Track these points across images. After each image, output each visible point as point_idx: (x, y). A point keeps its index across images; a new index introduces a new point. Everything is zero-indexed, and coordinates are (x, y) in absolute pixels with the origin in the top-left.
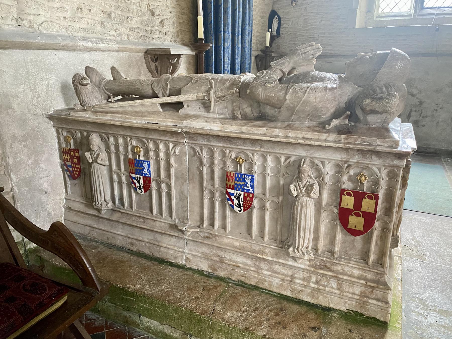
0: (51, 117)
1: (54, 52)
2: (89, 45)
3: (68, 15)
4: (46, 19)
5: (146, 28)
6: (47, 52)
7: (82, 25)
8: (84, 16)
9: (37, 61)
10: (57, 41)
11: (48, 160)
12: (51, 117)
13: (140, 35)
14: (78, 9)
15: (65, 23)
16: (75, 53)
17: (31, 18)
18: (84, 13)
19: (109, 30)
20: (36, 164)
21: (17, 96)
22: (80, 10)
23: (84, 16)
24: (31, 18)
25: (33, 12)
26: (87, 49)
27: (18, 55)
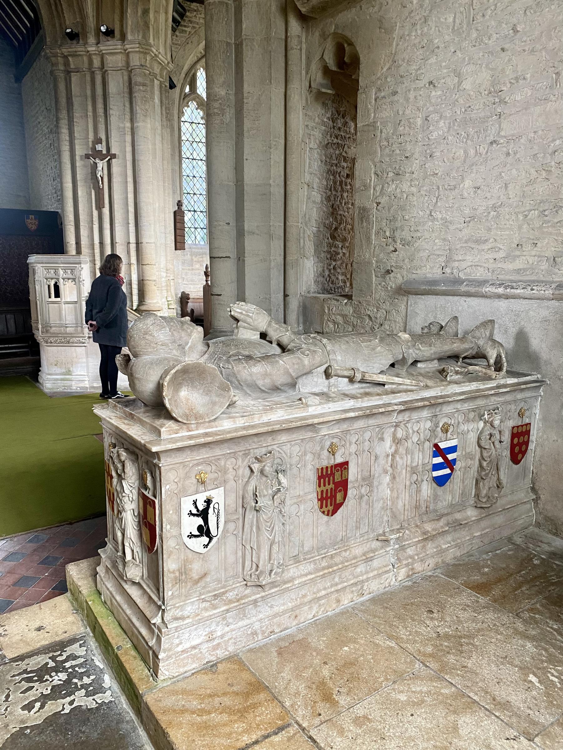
1: (464, 298)
2: (501, 290)
3: (502, 254)
4: (472, 264)
6: (456, 298)
7: (519, 264)
8: (525, 253)
16: (488, 301)
18: (524, 249)
22: (520, 247)
23: (525, 253)
24: (456, 264)
25: (460, 258)
26: (499, 296)
27: (431, 300)
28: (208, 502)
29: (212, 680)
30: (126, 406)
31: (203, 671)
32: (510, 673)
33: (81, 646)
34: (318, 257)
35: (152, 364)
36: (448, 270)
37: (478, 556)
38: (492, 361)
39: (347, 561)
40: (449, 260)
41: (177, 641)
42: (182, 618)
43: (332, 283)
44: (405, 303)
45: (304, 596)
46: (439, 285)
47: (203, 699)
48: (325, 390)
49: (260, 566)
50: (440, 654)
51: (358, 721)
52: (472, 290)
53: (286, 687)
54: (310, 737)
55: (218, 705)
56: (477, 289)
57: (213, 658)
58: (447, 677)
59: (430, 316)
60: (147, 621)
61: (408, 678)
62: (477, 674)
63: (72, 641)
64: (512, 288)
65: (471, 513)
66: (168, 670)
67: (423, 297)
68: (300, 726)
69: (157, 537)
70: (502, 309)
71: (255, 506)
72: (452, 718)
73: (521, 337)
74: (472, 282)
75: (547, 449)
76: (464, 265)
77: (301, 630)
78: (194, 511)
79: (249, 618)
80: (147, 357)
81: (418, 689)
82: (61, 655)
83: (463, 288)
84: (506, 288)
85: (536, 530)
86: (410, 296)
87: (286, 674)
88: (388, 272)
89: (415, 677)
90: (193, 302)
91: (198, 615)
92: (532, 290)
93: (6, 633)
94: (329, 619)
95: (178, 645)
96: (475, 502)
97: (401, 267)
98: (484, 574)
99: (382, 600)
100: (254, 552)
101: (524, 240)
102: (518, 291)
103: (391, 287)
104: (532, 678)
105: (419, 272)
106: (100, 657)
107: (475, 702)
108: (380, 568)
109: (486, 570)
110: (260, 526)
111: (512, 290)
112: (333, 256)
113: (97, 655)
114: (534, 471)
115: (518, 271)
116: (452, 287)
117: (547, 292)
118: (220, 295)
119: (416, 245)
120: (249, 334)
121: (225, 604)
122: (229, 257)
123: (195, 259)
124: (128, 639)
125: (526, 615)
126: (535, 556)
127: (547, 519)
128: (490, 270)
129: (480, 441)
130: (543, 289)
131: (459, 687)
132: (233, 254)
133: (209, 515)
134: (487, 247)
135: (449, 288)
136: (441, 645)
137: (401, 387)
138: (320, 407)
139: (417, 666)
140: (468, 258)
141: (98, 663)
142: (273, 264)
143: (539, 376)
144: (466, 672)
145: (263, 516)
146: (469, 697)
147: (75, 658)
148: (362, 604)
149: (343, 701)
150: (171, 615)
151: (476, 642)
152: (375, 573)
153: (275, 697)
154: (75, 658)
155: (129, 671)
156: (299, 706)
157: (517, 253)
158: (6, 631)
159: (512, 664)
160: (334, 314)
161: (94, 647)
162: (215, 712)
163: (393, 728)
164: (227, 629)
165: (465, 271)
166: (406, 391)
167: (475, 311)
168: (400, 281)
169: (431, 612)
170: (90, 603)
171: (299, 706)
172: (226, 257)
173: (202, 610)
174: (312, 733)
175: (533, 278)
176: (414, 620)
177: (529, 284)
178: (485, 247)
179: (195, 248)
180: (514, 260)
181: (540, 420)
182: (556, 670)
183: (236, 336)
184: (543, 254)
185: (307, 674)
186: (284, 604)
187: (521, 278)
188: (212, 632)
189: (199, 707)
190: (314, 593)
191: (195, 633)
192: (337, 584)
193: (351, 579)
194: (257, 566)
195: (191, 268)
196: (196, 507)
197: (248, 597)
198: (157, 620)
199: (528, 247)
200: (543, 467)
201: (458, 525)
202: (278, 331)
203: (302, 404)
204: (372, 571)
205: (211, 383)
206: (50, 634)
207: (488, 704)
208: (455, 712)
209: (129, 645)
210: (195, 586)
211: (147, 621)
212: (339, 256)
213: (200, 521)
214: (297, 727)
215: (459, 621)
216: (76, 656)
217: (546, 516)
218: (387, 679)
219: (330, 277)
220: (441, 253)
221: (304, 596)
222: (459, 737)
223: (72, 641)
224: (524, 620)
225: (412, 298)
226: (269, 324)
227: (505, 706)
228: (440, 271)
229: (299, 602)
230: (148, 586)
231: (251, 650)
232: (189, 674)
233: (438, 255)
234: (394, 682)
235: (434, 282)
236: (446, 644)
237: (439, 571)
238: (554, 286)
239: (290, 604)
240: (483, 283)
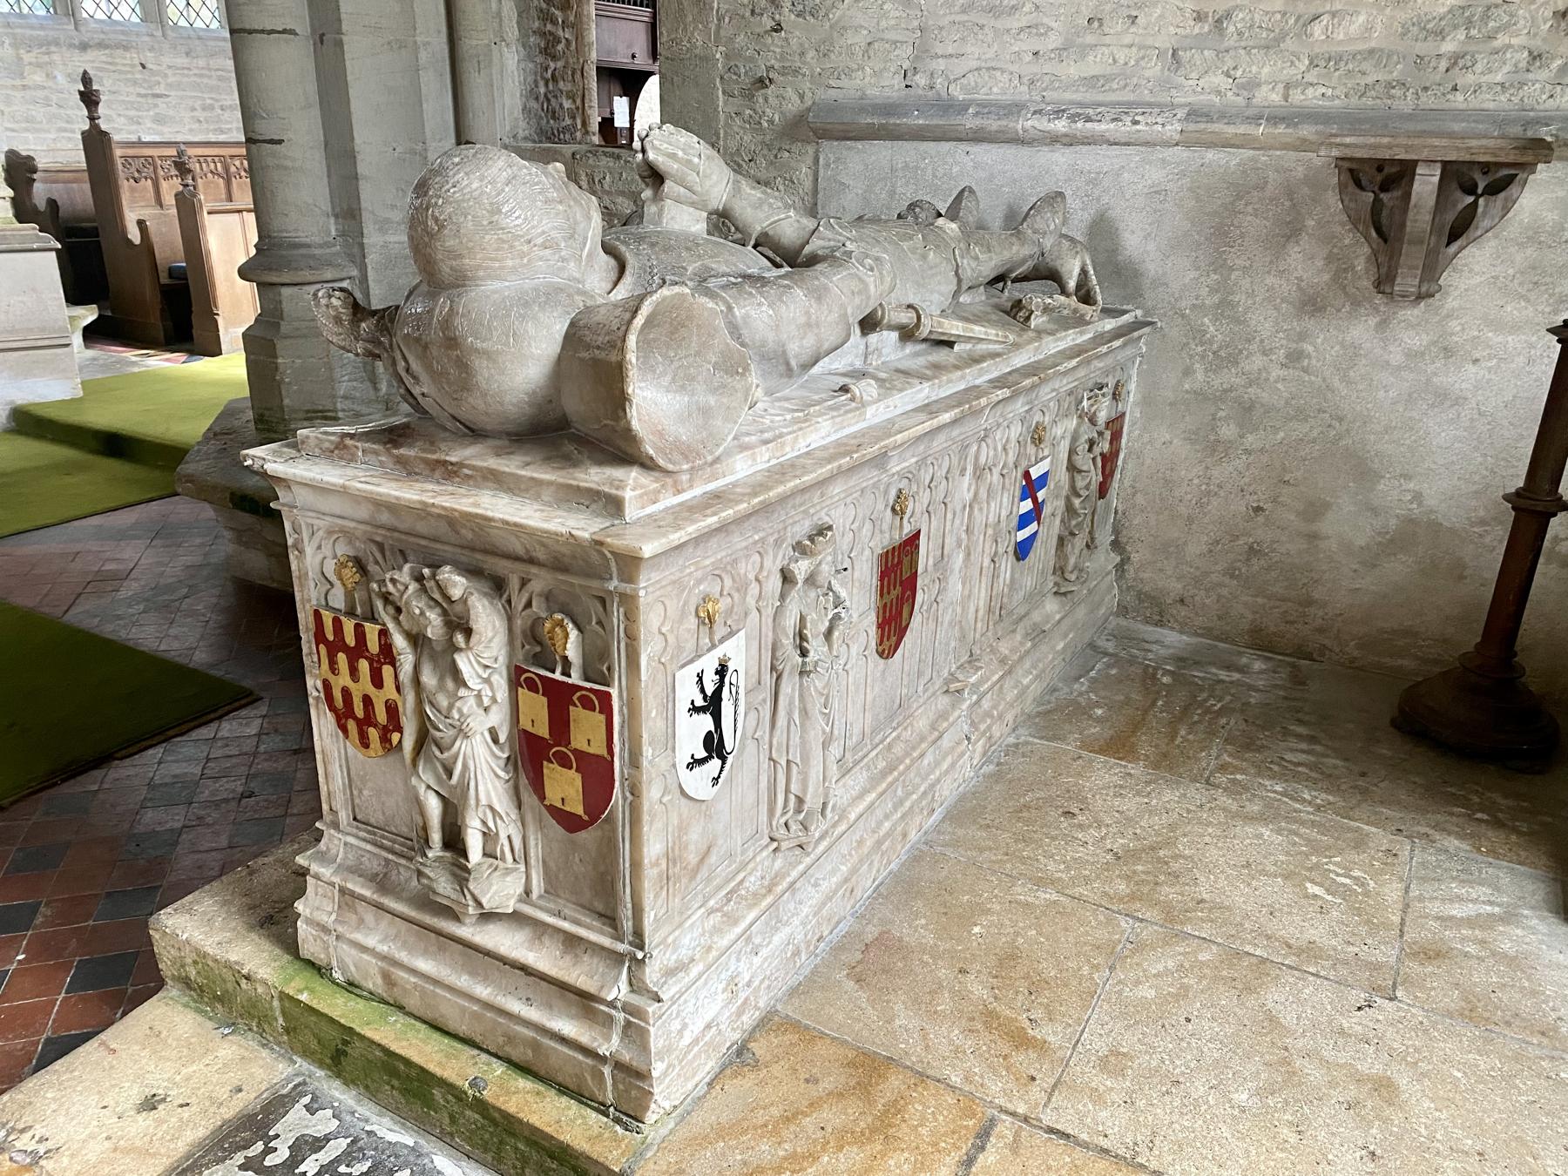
1: (964, 146)
2: (1061, 126)
3: (1054, 41)
4: (980, 66)
6: (945, 146)
7: (1094, 65)
8: (1107, 40)
9: (917, 168)
10: (958, 120)
13: (1370, 80)
18: (1107, 30)
19: (1194, 75)
22: (1096, 24)
24: (941, 64)
25: (950, 51)
26: (1054, 140)
27: (881, 153)
28: (722, 671)
29: (762, 1083)
30: (397, 445)
31: (728, 1071)
32: (1274, 890)
33: (310, 1109)
34: (524, 46)
35: (526, 304)
36: (921, 80)
37: (1066, 690)
38: (1072, 284)
39: (914, 748)
40: (922, 52)
41: (676, 1025)
42: (681, 967)
43: (554, 118)
44: (809, 161)
45: (860, 842)
46: (905, 115)
47: (776, 1131)
48: (858, 364)
49: (808, 798)
50: (1146, 890)
51: (1114, 1062)
52: (993, 124)
53: (927, 1046)
54: (1051, 1130)
55: (820, 1134)
56: (1004, 123)
57: (737, 1036)
58: (1188, 929)
59: (877, 190)
60: (585, 1002)
61: (1126, 953)
62: (1228, 908)
63: (276, 1106)
64: (1089, 120)
65: (1052, 606)
66: (667, 1098)
67: (859, 145)
68: (1013, 1114)
69: (617, 784)
70: (1057, 169)
71: (804, 664)
72: (1251, 1001)
73: (1102, 233)
74: (986, 108)
75: (1148, 461)
77: (863, 916)
78: (700, 702)
79: (787, 924)
80: (497, 285)
81: (1160, 967)
82: (269, 1151)
83: (970, 122)
84: (1073, 118)
85: (1123, 622)
86: (825, 143)
87: (904, 1018)
88: (762, 83)
89: (1139, 947)
90: (45, 181)
91: (709, 949)
92: (1136, 123)
93: (49, 1145)
94: (896, 877)
95: (680, 1032)
96: (1056, 584)
97: (796, 72)
98: (1099, 720)
99: (964, 812)
100: (794, 769)
101: (1108, 7)
102: (1103, 127)
103: (771, 122)
104: (1313, 889)
105: (845, 82)
106: (386, 1121)
107: (1263, 961)
108: (953, 748)
109: (1099, 712)
110: (809, 706)
111: (1089, 125)
112: (548, 51)
113: (374, 1118)
114: (1120, 508)
115: (1091, 81)
116: (942, 122)
117: (1168, 127)
118: (280, 142)
119: (835, 15)
120: (686, 217)
121: (750, 907)
122: (292, 32)
123: (27, 58)
124: (484, 1056)
125: (1221, 779)
126: (1156, 669)
127: (1142, 597)
128: (1025, 80)
129: (1075, 457)
130: (1159, 120)
131: (1219, 940)
132: (303, 27)
133: (723, 704)
134: (1016, 25)
135: (935, 122)
136: (1134, 872)
137: (982, 347)
138: (882, 405)
139: (1123, 924)
140: (969, 49)
141: (392, 1137)
142: (423, 56)
143: (1139, 313)
144: (1210, 910)
145: (816, 683)
146: (1248, 954)
147: (318, 1144)
148: (937, 829)
149: (1051, 1033)
150: (657, 968)
151: (1183, 847)
152: (949, 760)
153: (921, 1074)
154: (318, 1144)
155: (548, 1130)
156: (982, 1077)
157: (1090, 39)
158: (42, 1140)
159: (1264, 873)
160: (609, 193)
161: (351, 1102)
162: (824, 1150)
163: (1179, 1057)
164: (757, 960)
165: (964, 81)
166: (994, 355)
167: (991, 177)
168: (793, 105)
169: (1068, 814)
170: (304, 997)
171: (982, 1077)
172: (284, 31)
173: (711, 935)
174: (1048, 1119)
176: (1054, 838)
177: (1124, 109)
178: (1015, 23)
179: (21, 27)
180: (1083, 56)
181: (1136, 404)
182: (1335, 864)
183: (658, 223)
184: (1149, 42)
185: (944, 1004)
186: (833, 872)
187: (1100, 98)
188: (732, 978)
189: (781, 1153)
190: (874, 832)
191: (704, 993)
192: (901, 802)
193: (919, 786)
194: (800, 801)
195: (18, 82)
196: (702, 690)
197: (783, 877)
198: (619, 990)
199: (1116, 26)
200: (1140, 499)
201: (1039, 634)
202: (766, 208)
203: (853, 399)
204: (944, 759)
205: (698, 354)
206: (194, 1109)
207: (1285, 956)
208: (1249, 989)
209: (499, 1069)
210: (694, 884)
211: (585, 1002)
212: (560, 47)
213: (707, 722)
214: (1010, 1119)
215: (1128, 819)
216: (317, 1139)
217: (1140, 593)
218: (1096, 967)
219: (548, 100)
220: (899, 38)
221: (860, 842)
222: (1287, 1031)
223: (276, 1106)
224: (1225, 790)
225: (829, 150)
226: (737, 190)
227: (1310, 951)
228: (898, 82)
229: (856, 858)
230: (559, 914)
231: (794, 992)
232: (702, 1089)
233: (895, 42)
234: (1112, 968)
235: (888, 109)
236: (1140, 868)
237: (1021, 731)
238: (1181, 114)
239: (844, 868)
240: (1015, 109)
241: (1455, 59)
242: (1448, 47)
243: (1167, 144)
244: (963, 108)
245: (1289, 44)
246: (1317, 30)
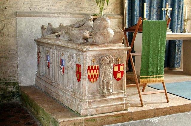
0: (35, 40)
2: (56, 15)
3: (50, 4)
4: (42, 7)
5: (92, 7)
7: (56, 8)
11: (32, 56)
12: (35, 40)
14: (55, 2)
15: (49, 8)
17: (35, 7)
20: (28, 56)
21: (25, 32)
26: (54, 17)
27: (28, 19)
64: (59, 14)
74: (44, 13)
76: (38, 7)
115: (56, 10)
175: (61, 11)
240: (48, 13)
241: (94, 8)
242: (93, 7)
243: (68, 17)
244: (41, 13)
245: (78, 6)
246: (81, 4)
